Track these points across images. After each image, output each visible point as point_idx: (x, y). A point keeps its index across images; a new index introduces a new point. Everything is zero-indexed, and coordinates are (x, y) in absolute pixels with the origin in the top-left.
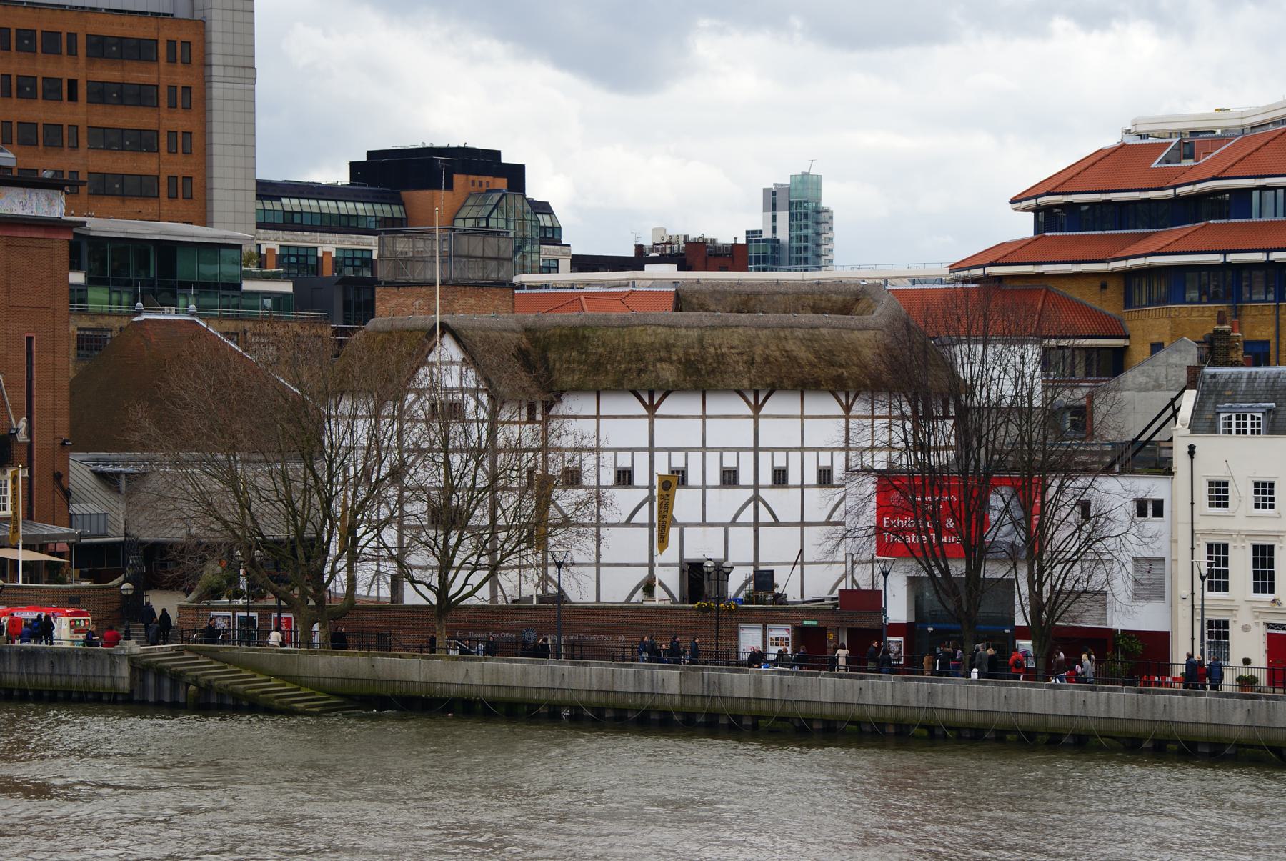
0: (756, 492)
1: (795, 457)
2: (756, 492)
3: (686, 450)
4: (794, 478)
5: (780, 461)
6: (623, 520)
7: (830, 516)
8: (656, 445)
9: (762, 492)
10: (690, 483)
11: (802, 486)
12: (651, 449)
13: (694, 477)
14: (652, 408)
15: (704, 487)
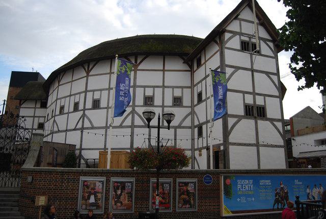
0: (134, 110)
1: (158, 91)
2: (134, 110)
3: (101, 90)
4: (158, 101)
5: (149, 92)
6: (74, 128)
7: (181, 123)
8: (88, 89)
9: (136, 109)
10: (101, 106)
11: (163, 106)
12: (86, 91)
13: (103, 104)
14: (88, 72)
15: (108, 108)
